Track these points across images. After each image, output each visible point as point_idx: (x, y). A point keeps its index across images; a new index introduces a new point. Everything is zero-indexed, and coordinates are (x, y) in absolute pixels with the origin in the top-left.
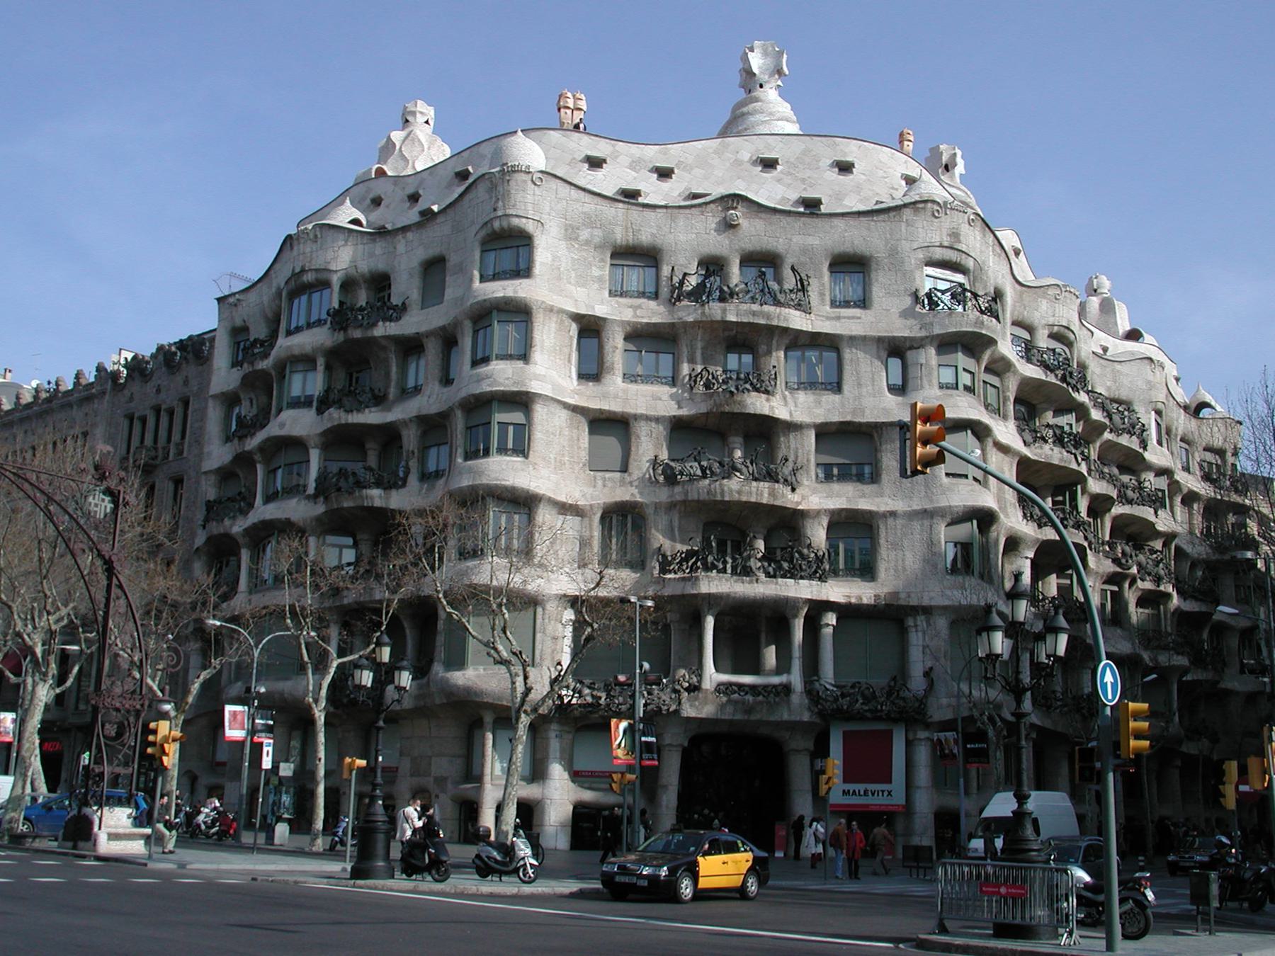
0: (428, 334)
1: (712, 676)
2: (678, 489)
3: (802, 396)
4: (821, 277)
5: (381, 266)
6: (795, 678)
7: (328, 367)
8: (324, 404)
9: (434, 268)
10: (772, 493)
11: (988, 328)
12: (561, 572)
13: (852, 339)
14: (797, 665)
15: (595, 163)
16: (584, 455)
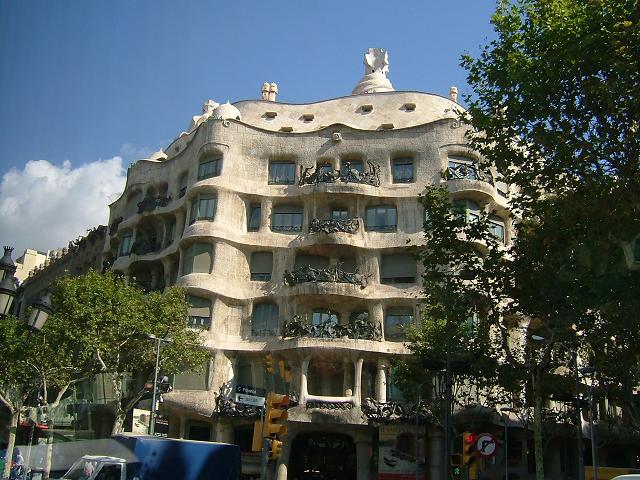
0: (178, 211)
1: (306, 395)
2: (294, 288)
3: (374, 234)
4: (385, 166)
5: (164, 179)
6: (357, 399)
7: (139, 234)
8: (135, 250)
9: (184, 176)
10: (347, 289)
11: (484, 189)
12: (225, 335)
13: (403, 199)
14: (358, 390)
15: (270, 116)
16: (248, 272)
